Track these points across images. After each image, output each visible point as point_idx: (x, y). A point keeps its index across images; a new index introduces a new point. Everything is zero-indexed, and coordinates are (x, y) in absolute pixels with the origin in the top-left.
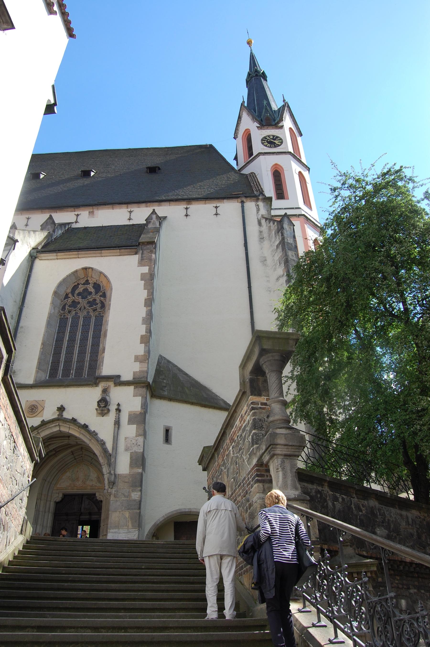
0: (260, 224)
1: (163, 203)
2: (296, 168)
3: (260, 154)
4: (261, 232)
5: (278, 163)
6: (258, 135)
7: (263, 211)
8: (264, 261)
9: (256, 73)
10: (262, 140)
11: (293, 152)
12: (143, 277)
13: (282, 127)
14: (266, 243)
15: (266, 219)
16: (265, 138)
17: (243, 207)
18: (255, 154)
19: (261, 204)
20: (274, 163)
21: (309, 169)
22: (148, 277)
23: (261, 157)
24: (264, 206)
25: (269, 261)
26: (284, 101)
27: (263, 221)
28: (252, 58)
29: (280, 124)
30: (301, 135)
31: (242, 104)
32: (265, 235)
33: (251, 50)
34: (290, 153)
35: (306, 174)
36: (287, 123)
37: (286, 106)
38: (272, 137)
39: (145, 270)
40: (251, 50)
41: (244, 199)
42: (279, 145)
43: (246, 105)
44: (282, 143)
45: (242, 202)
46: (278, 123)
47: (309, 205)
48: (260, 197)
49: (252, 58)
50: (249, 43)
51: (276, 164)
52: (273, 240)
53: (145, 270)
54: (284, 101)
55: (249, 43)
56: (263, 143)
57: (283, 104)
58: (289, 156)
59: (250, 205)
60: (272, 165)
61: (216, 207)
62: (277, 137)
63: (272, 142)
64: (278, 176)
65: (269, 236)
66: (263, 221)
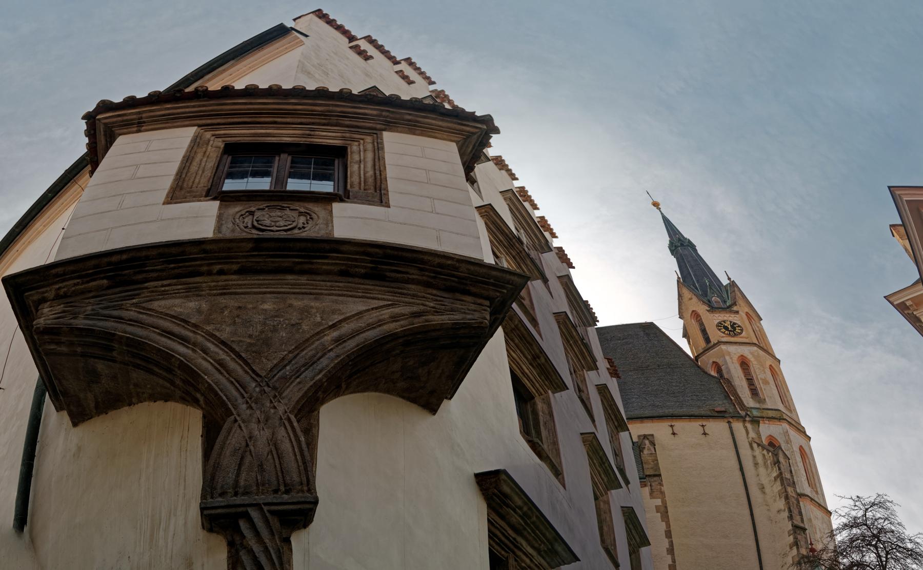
0: (752, 448)
1: (646, 420)
4: (754, 457)
6: (712, 320)
7: (752, 434)
8: (762, 488)
12: (658, 509)
14: (762, 470)
15: (759, 445)
17: (731, 428)
19: (749, 425)
22: (662, 509)
24: (753, 429)
25: (767, 490)
27: (755, 445)
29: (735, 308)
32: (760, 460)
39: (658, 502)
41: (731, 420)
45: (729, 422)
48: (747, 419)
52: (770, 470)
53: (658, 502)
59: (738, 426)
61: (703, 426)
62: (735, 324)
65: (765, 463)
66: (755, 445)
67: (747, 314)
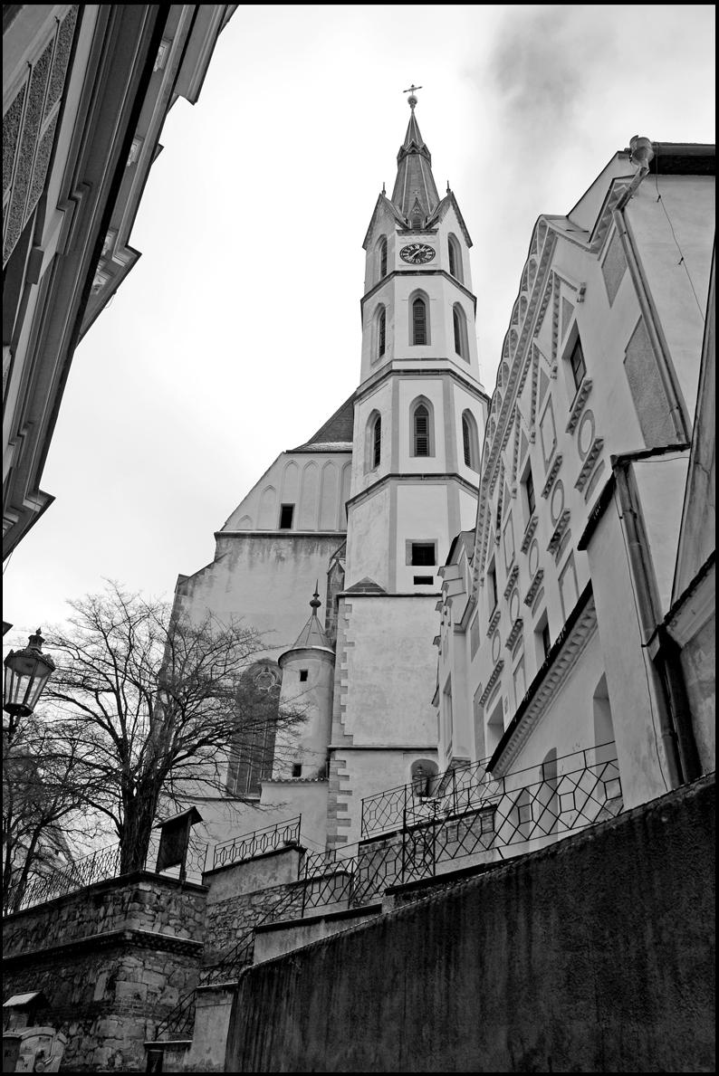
2: (452, 294)
3: (396, 273)
5: (423, 289)
6: (399, 242)
9: (413, 148)
10: (402, 252)
11: (449, 273)
13: (436, 231)
16: (407, 248)
18: (389, 272)
20: (416, 288)
21: (476, 299)
23: (397, 279)
26: (448, 190)
28: (413, 125)
29: (433, 228)
30: (470, 245)
31: (382, 197)
33: (413, 113)
34: (441, 272)
35: (467, 304)
36: (447, 224)
37: (451, 197)
38: (418, 247)
40: (413, 113)
42: (429, 260)
43: (389, 196)
44: (433, 256)
46: (431, 224)
47: (466, 358)
49: (413, 125)
50: (413, 102)
51: (419, 290)
54: (448, 190)
55: (413, 102)
56: (402, 257)
57: (446, 195)
58: (442, 278)
60: (411, 291)
63: (418, 255)
64: (419, 303)
67: (452, 237)
